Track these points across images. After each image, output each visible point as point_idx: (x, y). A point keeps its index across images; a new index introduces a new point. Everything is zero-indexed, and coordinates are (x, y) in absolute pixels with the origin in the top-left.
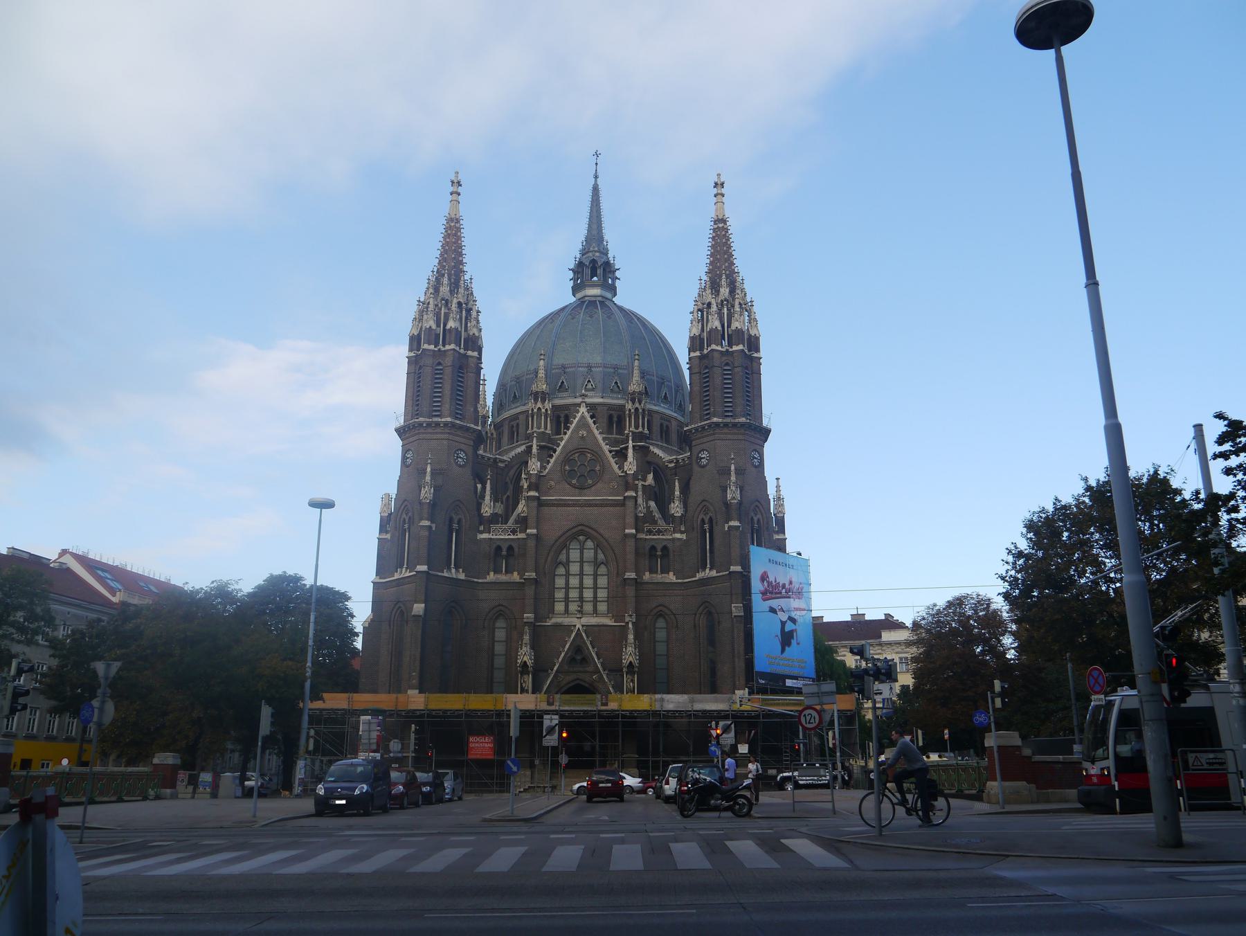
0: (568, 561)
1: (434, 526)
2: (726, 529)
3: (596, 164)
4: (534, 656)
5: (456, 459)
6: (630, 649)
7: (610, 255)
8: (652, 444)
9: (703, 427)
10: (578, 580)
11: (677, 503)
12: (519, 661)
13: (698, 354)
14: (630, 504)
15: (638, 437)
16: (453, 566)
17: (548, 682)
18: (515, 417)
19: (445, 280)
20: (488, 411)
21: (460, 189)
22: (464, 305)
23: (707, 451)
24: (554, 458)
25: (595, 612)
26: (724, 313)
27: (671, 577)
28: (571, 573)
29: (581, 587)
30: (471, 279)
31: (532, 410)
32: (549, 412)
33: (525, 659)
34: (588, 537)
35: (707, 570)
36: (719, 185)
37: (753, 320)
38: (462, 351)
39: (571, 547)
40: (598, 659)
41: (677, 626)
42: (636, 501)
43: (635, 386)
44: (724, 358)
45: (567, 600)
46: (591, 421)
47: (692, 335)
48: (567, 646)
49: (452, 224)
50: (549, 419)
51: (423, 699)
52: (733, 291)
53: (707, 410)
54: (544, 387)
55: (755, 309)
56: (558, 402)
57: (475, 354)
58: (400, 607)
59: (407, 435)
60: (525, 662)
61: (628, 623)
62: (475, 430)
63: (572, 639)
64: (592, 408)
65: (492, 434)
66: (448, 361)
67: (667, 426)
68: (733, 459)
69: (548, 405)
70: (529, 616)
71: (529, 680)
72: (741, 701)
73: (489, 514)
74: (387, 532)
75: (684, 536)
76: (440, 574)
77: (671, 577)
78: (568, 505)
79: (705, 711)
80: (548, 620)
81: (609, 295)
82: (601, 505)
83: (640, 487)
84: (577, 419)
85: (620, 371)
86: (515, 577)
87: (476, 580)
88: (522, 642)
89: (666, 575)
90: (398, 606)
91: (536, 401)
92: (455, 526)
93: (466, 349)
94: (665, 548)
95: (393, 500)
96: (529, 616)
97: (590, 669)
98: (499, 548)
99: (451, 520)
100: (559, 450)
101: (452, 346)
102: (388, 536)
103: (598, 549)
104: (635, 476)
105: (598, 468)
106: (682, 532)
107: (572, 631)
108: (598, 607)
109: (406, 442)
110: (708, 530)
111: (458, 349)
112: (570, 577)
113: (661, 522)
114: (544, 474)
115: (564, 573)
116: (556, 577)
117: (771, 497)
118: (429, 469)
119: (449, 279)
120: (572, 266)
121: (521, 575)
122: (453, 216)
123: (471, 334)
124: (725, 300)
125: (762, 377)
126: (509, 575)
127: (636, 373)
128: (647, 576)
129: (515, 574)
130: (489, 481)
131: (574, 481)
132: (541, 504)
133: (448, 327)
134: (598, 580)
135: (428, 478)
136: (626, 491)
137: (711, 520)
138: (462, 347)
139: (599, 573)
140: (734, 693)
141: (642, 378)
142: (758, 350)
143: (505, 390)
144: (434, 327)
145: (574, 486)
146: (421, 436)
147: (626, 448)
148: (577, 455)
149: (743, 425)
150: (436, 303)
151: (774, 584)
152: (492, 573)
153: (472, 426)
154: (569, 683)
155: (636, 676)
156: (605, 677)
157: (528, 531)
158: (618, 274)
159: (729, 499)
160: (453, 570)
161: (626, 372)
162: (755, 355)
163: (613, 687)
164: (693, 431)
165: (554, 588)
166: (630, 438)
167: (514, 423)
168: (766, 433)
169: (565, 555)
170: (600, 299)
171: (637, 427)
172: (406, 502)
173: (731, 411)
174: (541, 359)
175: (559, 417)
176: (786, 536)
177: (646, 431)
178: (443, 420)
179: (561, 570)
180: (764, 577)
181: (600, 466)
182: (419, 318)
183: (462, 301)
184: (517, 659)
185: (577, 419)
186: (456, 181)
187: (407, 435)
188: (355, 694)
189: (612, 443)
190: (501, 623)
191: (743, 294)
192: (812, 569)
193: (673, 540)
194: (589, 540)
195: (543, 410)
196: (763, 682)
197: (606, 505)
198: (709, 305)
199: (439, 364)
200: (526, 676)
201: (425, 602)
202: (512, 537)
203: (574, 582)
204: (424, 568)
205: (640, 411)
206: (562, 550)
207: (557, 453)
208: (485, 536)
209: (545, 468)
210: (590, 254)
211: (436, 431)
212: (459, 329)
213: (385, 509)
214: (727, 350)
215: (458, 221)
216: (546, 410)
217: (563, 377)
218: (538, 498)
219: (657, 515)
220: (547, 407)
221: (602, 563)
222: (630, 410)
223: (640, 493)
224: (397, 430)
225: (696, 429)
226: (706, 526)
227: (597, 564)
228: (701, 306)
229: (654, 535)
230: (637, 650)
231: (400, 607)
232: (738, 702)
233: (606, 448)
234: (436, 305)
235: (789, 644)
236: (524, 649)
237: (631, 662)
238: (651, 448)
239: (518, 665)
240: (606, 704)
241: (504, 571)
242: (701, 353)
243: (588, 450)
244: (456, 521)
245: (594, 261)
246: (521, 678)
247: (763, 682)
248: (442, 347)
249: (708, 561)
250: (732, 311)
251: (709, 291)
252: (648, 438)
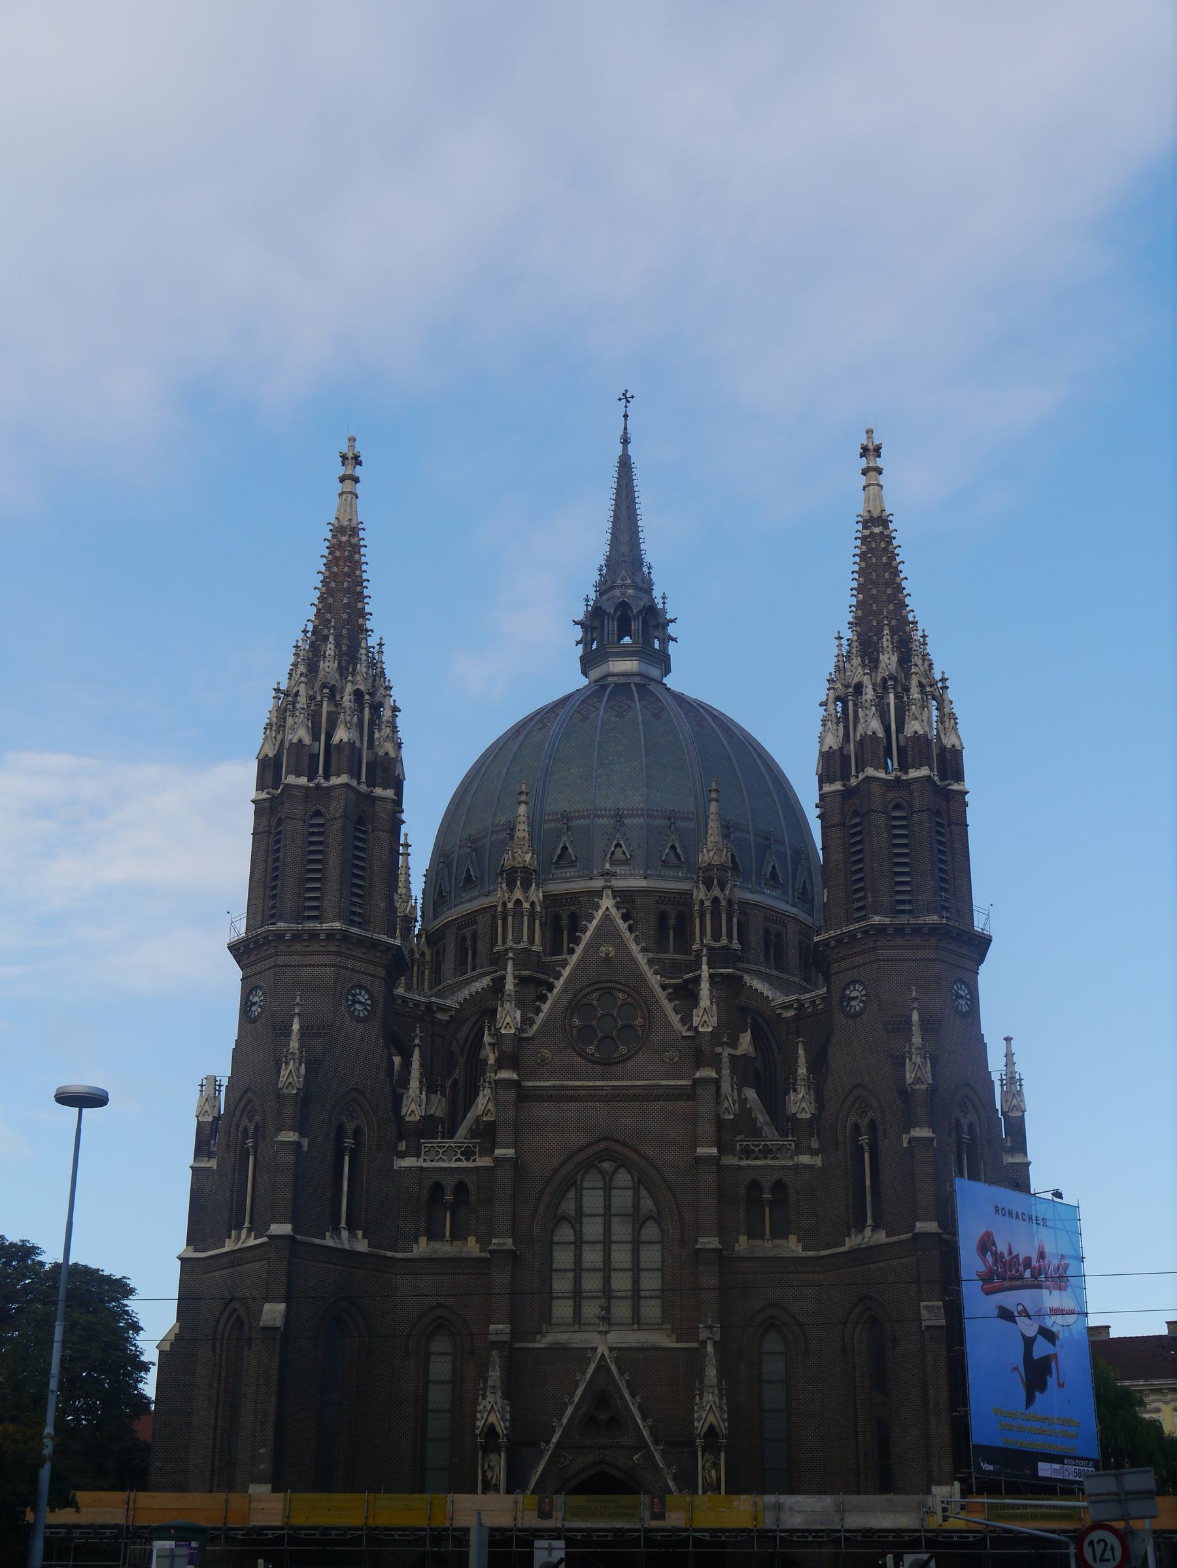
0: (580, 1214)
1: (305, 1142)
2: (905, 1145)
3: (626, 416)
4: (511, 1413)
5: (350, 1006)
6: (710, 1398)
7: (657, 593)
8: (748, 971)
9: (852, 936)
10: (601, 1254)
11: (802, 1092)
12: (480, 1424)
13: (837, 786)
14: (705, 1095)
15: (719, 957)
16: (343, 1224)
17: (540, 1469)
18: (469, 920)
19: (330, 649)
20: (414, 908)
21: (359, 471)
22: (367, 697)
23: (860, 983)
24: (549, 1003)
25: (636, 1320)
26: (888, 704)
27: (793, 1247)
28: (585, 1238)
29: (607, 1269)
30: (381, 645)
31: (504, 904)
32: (538, 909)
33: (492, 1419)
34: (622, 1163)
35: (868, 1232)
36: (870, 451)
37: (947, 718)
38: (363, 788)
39: (585, 1185)
40: (644, 1419)
42: (718, 1089)
43: (711, 853)
44: (891, 795)
45: (577, 1296)
46: (623, 926)
47: (825, 749)
48: (579, 1393)
49: (344, 539)
50: (537, 922)
51: (280, 1505)
52: (905, 660)
53: (859, 900)
54: (528, 857)
55: (951, 694)
56: (555, 888)
57: (390, 793)
58: (235, 1310)
59: (252, 958)
60: (492, 1426)
61: (704, 1343)
62: (389, 947)
63: (588, 1376)
64: (625, 898)
65: (423, 954)
66: (335, 808)
67: (778, 935)
68: (915, 999)
69: (536, 895)
70: (500, 1329)
71: (499, 1465)
72: (945, 1510)
73: (417, 1118)
74: (210, 1155)
75: (818, 1161)
76: (317, 1241)
77: (793, 1247)
78: (580, 1099)
79: (869, 1530)
80: (538, 1337)
81: (654, 672)
82: (646, 1098)
83: (725, 1059)
84: (595, 922)
85: (681, 824)
86: (471, 1248)
87: (390, 1254)
88: (485, 1382)
89: (783, 1242)
90: (230, 1307)
91: (511, 885)
92: (349, 1142)
93: (371, 783)
94: (779, 1186)
95: (223, 1089)
96: (500, 1329)
98: (437, 1188)
99: (340, 1130)
100: (559, 985)
101: (344, 779)
102: (213, 1164)
103: (644, 1193)
104: (715, 1035)
105: (639, 1021)
106: (813, 1153)
107: (589, 1361)
108: (642, 1309)
109: (250, 971)
111: (354, 783)
112: (585, 1247)
113: (769, 1132)
114: (530, 1036)
115: (572, 1239)
116: (555, 1247)
117: (995, 1077)
118: (296, 1027)
119: (338, 646)
120: (580, 616)
121: (483, 1243)
122: (345, 523)
123: (381, 752)
124: (891, 679)
126: (458, 1245)
127: (713, 826)
128: (743, 1245)
129: (472, 1240)
130: (417, 1051)
131: (591, 1049)
132: (523, 1095)
133: (336, 740)
134: (642, 1254)
135: (294, 1044)
136: (698, 1067)
137: (873, 1127)
138: (363, 779)
139: (643, 1238)
140: (929, 1492)
141: (726, 836)
142: (959, 776)
143: (449, 865)
144: (307, 740)
145: (590, 1059)
146: (281, 960)
147: (697, 980)
148: (595, 995)
149: (934, 929)
150: (311, 693)
151: (1007, 1258)
152: (423, 1240)
153: (384, 937)
155: (723, 1455)
156: (658, 1457)
157: (498, 1152)
158: (672, 630)
159: (909, 1081)
160: (345, 1234)
161: (692, 825)
162: (955, 787)
163: (674, 1480)
164: (833, 943)
165: (552, 1270)
166: (705, 959)
167: (468, 932)
168: (982, 943)
169: (573, 1201)
170: (637, 679)
171: (716, 937)
172: (249, 1095)
173: (909, 902)
174: (520, 803)
175: (557, 918)
176: (1030, 1158)
177: (736, 945)
178: (325, 926)
179: (565, 1233)
180: (986, 1245)
181: (644, 1018)
182: (278, 724)
183: (362, 688)
184: (475, 1419)
185: (595, 922)
186: (350, 455)
187: (252, 958)
188: (139, 1494)
189: (665, 970)
190: (442, 1344)
191: (926, 666)
192: (1085, 1227)
193: (797, 1168)
194: (622, 1170)
195: (526, 905)
196: (991, 1468)
197: (658, 1098)
198: (859, 688)
199: (318, 814)
200: (493, 1456)
201: (288, 1300)
202: (464, 1164)
203: (592, 1256)
204: (285, 1229)
205: (724, 903)
206: (569, 1189)
207: (555, 991)
208: (408, 1162)
209: (531, 1022)
210: (617, 592)
211: (309, 949)
212: (358, 745)
213: (207, 1108)
214: (898, 779)
215: (354, 532)
216: (533, 904)
217: (565, 838)
218: (517, 1084)
219: (761, 1117)
220: (533, 898)
221: (650, 1217)
222: (702, 902)
223: (726, 1072)
224: (232, 948)
225: (839, 940)
226: (864, 1139)
227: (638, 1220)
228: (841, 691)
229: (757, 1158)
230: (725, 1401)
231: (235, 1310)
232: (939, 1511)
233: (655, 980)
234: (312, 698)
235: (1042, 1387)
236: (490, 1397)
237: (711, 1426)
238: (747, 978)
239: (478, 1432)
240: (661, 1516)
241: (448, 1234)
242: (844, 785)
243: (617, 986)
244: (350, 1132)
245: (623, 606)
246: (483, 1458)
247: (991, 1468)
248: (322, 781)
249: (869, 1213)
250: (905, 699)
251: (856, 661)
252: (740, 959)
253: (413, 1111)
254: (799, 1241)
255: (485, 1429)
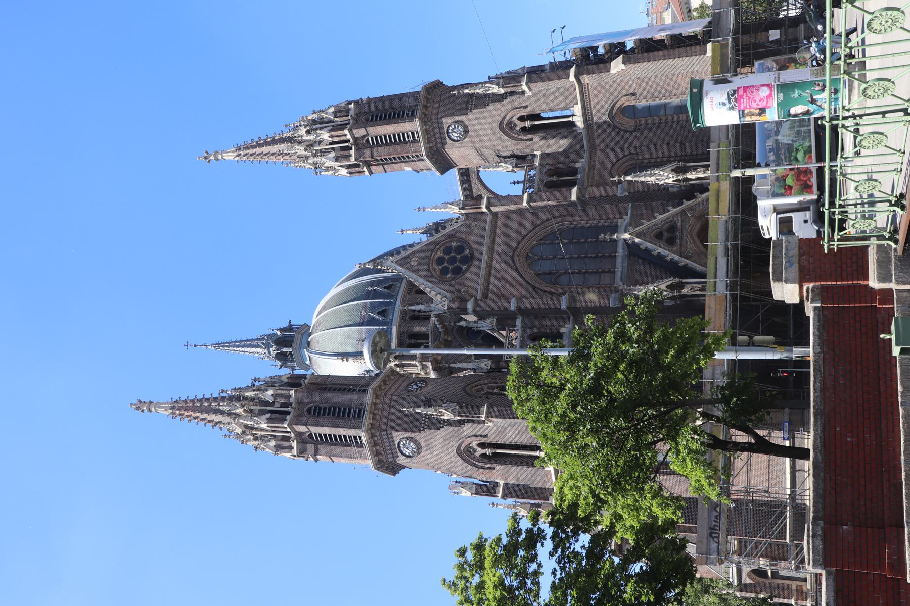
33: (663, 287)
35: (575, 119)
41: (637, 154)
97: (679, 220)
110: (533, 123)
125: (386, 95)
154: (695, 244)
218: (476, 301)
253: (485, 365)
254: (579, 162)
255: (669, 290)
